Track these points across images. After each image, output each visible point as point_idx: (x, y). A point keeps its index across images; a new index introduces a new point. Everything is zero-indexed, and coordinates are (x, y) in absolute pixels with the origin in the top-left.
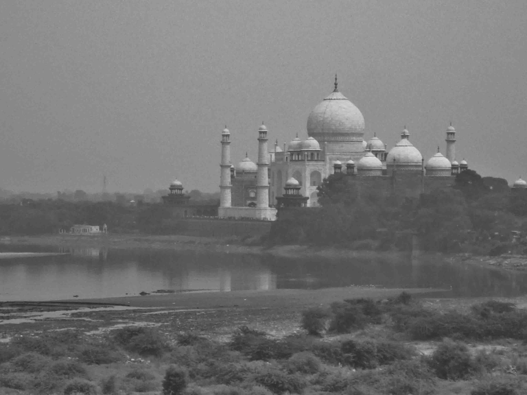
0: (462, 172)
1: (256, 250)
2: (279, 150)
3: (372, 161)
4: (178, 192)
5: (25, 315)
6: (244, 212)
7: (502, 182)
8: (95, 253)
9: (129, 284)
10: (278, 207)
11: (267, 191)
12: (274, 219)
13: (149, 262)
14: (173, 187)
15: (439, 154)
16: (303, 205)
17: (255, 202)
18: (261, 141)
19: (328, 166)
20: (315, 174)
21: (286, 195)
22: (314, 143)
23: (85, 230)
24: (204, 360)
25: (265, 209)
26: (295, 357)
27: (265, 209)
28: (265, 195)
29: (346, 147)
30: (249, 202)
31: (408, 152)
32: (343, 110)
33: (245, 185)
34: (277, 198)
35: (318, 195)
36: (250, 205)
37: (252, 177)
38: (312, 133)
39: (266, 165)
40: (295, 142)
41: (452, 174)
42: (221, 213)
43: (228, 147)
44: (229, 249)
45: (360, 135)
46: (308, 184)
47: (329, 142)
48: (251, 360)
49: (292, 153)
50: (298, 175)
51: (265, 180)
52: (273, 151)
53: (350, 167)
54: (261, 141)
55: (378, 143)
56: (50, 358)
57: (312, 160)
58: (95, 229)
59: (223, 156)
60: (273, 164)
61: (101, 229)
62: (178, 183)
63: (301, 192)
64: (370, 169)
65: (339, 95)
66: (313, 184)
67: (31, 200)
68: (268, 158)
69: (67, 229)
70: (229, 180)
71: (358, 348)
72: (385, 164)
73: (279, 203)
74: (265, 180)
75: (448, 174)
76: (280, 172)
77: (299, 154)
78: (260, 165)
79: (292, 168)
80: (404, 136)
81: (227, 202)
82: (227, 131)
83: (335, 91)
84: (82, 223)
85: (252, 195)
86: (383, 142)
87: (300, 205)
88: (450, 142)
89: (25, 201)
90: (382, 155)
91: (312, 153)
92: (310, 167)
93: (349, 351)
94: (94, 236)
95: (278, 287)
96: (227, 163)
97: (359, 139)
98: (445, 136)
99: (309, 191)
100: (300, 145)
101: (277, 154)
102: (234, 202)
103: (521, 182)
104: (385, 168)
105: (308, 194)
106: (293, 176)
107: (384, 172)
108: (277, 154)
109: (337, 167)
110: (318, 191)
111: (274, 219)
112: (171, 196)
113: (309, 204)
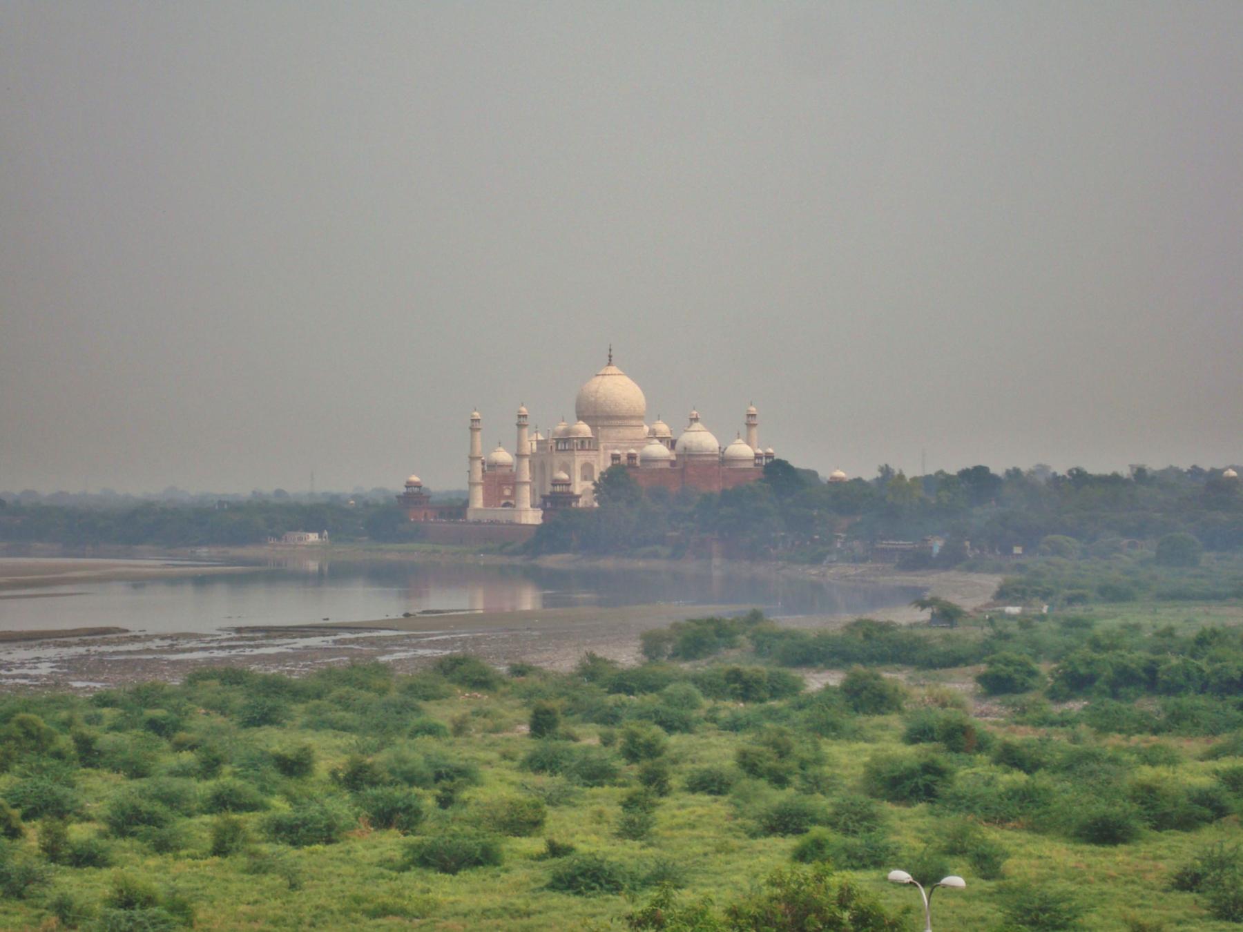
0: (767, 466)
1: (517, 560)
2: (540, 438)
3: (659, 450)
4: (416, 490)
5: (188, 646)
6: (501, 514)
7: (814, 474)
8: (313, 566)
9: (361, 605)
11: (528, 487)
12: (539, 521)
13: (381, 575)
14: (409, 485)
15: (740, 441)
16: (574, 504)
17: (512, 501)
18: (520, 426)
19: (602, 456)
20: (587, 469)
21: (553, 493)
22: (584, 429)
23: (300, 539)
24: (564, 694)
25: (527, 510)
26: (669, 689)
27: (527, 510)
28: (526, 494)
29: (628, 433)
30: (503, 502)
31: (703, 439)
32: (619, 388)
33: (500, 482)
34: (544, 497)
35: (594, 492)
36: (505, 505)
37: (507, 471)
38: (581, 417)
39: (526, 456)
40: (561, 427)
41: (756, 465)
42: (471, 516)
43: (478, 434)
44: (483, 559)
45: (640, 417)
46: (578, 478)
47: (603, 427)
48: (609, 693)
49: (558, 441)
50: (566, 468)
51: (526, 476)
52: (534, 438)
53: (631, 457)
54: (520, 426)
55: (663, 428)
56: (371, 695)
57: (583, 449)
58: (313, 537)
59: (472, 446)
61: (320, 537)
62: (415, 479)
63: (571, 489)
64: (656, 460)
65: (613, 369)
66: (585, 478)
67: (228, 503)
68: (530, 446)
69: (279, 539)
70: (480, 474)
71: (745, 677)
72: (674, 453)
73: (545, 503)
74: (526, 476)
75: (750, 465)
76: (543, 466)
77: (566, 442)
78: (519, 456)
79: (559, 459)
80: (696, 420)
81: (478, 502)
82: (477, 415)
83: (609, 364)
84: (296, 529)
85: (507, 493)
86: (670, 427)
87: (570, 504)
88: (750, 426)
89: (221, 503)
90: (672, 444)
91: (583, 440)
92: (579, 459)
93: (735, 681)
94: (313, 546)
95: (545, 606)
96: (477, 454)
97: (641, 422)
98: (745, 420)
99: (581, 486)
100: (568, 432)
101: (538, 442)
102: (487, 502)
103: (840, 474)
104: (673, 458)
105: (577, 491)
106: (560, 469)
107: (673, 463)
108: (538, 442)
109: (615, 457)
110: (593, 488)
111: (539, 521)
112: (406, 494)
113: (581, 504)
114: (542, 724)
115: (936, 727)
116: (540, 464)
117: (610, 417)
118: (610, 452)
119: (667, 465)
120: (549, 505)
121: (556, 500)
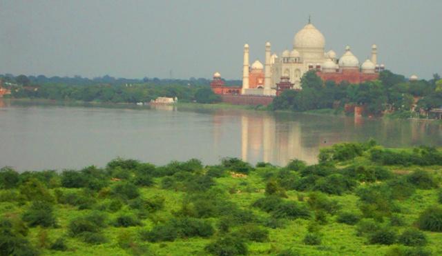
0: (381, 73)
6: (256, 92)
10: (277, 90)
16: (291, 88)
30: (258, 86)
31: (349, 60)
34: (277, 84)
35: (301, 82)
42: (243, 92)
51: (268, 73)
53: (318, 67)
58: (171, 100)
60: (273, 65)
61: (174, 100)
65: (311, 26)
72: (337, 65)
76: (277, 69)
79: (284, 67)
92: (294, 67)
104: (338, 68)
105: (292, 82)
107: (337, 70)
109: (310, 67)
111: (275, 95)
114: (270, 190)
115: (318, 199)
116: (276, 69)
117: (308, 48)
118: (308, 64)
119: (335, 71)
120: (279, 88)
121: (284, 86)
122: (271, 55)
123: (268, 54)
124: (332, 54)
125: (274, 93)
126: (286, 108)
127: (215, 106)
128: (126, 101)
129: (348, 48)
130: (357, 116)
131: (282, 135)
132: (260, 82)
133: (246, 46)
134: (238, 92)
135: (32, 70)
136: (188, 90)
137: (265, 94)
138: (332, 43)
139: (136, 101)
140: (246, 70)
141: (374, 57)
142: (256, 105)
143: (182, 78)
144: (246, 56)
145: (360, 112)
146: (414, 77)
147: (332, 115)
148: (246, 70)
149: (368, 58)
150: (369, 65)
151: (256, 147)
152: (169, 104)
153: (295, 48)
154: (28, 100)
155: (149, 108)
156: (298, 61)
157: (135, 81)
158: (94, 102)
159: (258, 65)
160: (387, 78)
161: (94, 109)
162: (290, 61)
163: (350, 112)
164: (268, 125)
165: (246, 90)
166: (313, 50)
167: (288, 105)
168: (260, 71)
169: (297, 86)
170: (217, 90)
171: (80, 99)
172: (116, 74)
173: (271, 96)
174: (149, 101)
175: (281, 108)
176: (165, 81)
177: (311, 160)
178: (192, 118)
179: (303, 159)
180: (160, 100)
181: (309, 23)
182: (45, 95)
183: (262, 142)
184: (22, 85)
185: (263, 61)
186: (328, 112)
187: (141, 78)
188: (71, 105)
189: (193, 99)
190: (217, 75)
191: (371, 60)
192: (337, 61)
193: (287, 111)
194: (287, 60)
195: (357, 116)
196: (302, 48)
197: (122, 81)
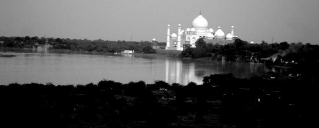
42: (167, 49)
58: (131, 52)
109: (200, 36)
116: (183, 37)
117: (199, 27)
121: (187, 46)
122: (181, 30)
123: (179, 30)
124: (211, 30)
125: (182, 49)
126: (188, 56)
127: (152, 55)
128: (109, 51)
129: (219, 27)
130: (223, 61)
131: (185, 71)
132: (175, 43)
133: (169, 25)
134: (164, 48)
135: (63, 36)
136: (139, 47)
137: (177, 49)
138: (212, 25)
139: (114, 52)
140: (168, 37)
141: (232, 32)
142: (173, 56)
143: (137, 41)
144: (169, 30)
145: (225, 59)
146: (252, 42)
147: (211, 60)
148: (168, 37)
149: (229, 32)
150: (230, 37)
151: (173, 75)
152: (131, 54)
153: (193, 27)
154: (61, 50)
155: (120, 55)
156: (194, 33)
157: (114, 42)
158: (93, 52)
159: (174, 35)
160: (239, 43)
161: (94, 56)
162: (190, 33)
163: (220, 60)
164: (179, 65)
165: (168, 47)
166: (201, 29)
167: (189, 55)
168: (176, 40)
169: (194, 46)
170: (154, 47)
171: (86, 50)
172: (105, 39)
173: (180, 51)
174: (120, 52)
175: (186, 57)
176: (128, 42)
177: (199, 82)
178: (141, 61)
179: (195, 82)
180: (126, 52)
181: (200, 14)
182: (69, 48)
183: (176, 71)
184: (58, 43)
185: (177, 33)
186: (209, 59)
187: (117, 40)
188: (82, 53)
189: (141, 51)
190: (154, 40)
191: (231, 33)
192: (214, 34)
193: (188, 58)
194: (189, 33)
195: (223, 61)
196: (196, 27)
197: (107, 42)
